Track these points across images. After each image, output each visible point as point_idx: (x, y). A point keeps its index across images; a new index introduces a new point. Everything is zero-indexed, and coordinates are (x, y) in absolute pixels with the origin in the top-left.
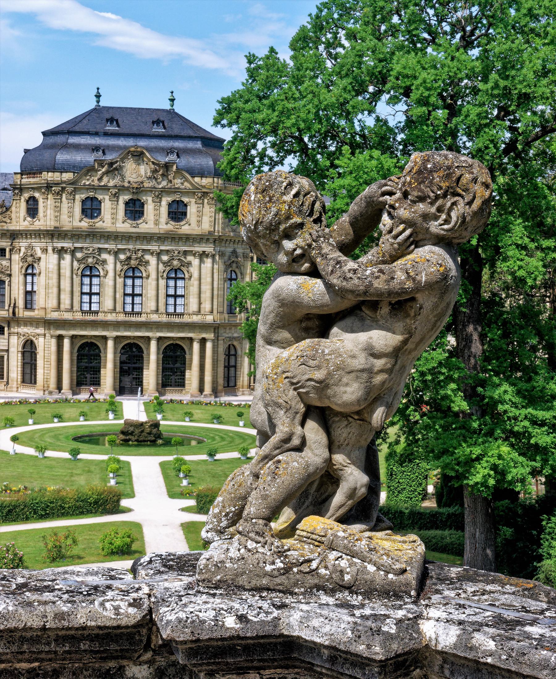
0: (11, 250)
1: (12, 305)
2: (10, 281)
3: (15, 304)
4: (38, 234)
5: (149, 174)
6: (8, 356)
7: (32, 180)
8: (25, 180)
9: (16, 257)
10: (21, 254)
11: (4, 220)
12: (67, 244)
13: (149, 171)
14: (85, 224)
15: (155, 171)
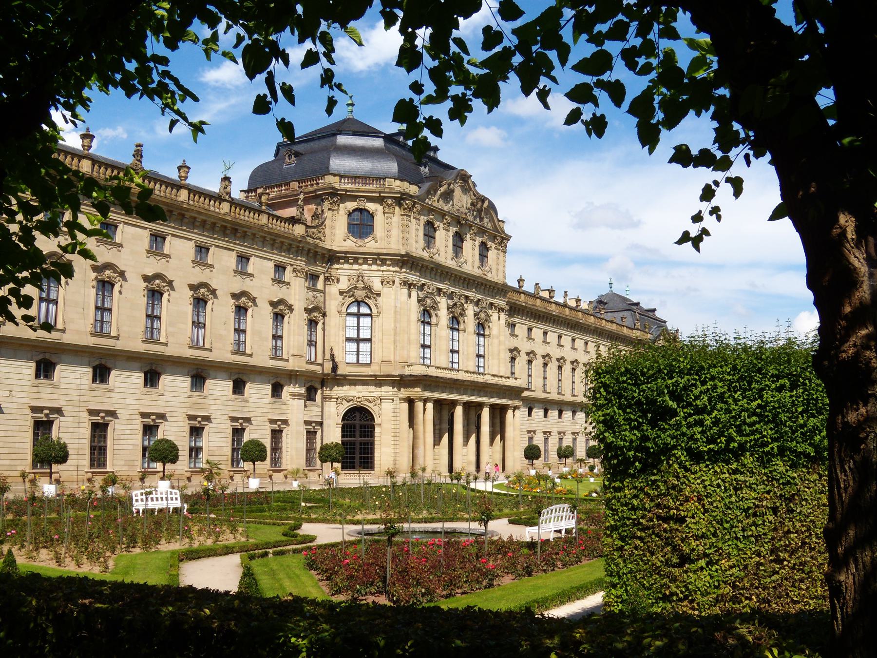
0: (327, 279)
1: (328, 357)
2: (324, 323)
3: (332, 355)
4: (380, 259)
5: (469, 206)
6: (322, 431)
7: (361, 187)
8: (343, 186)
9: (333, 290)
10: (344, 285)
11: (319, 235)
12: (413, 277)
13: (470, 201)
14: (425, 255)
15: (472, 204)
